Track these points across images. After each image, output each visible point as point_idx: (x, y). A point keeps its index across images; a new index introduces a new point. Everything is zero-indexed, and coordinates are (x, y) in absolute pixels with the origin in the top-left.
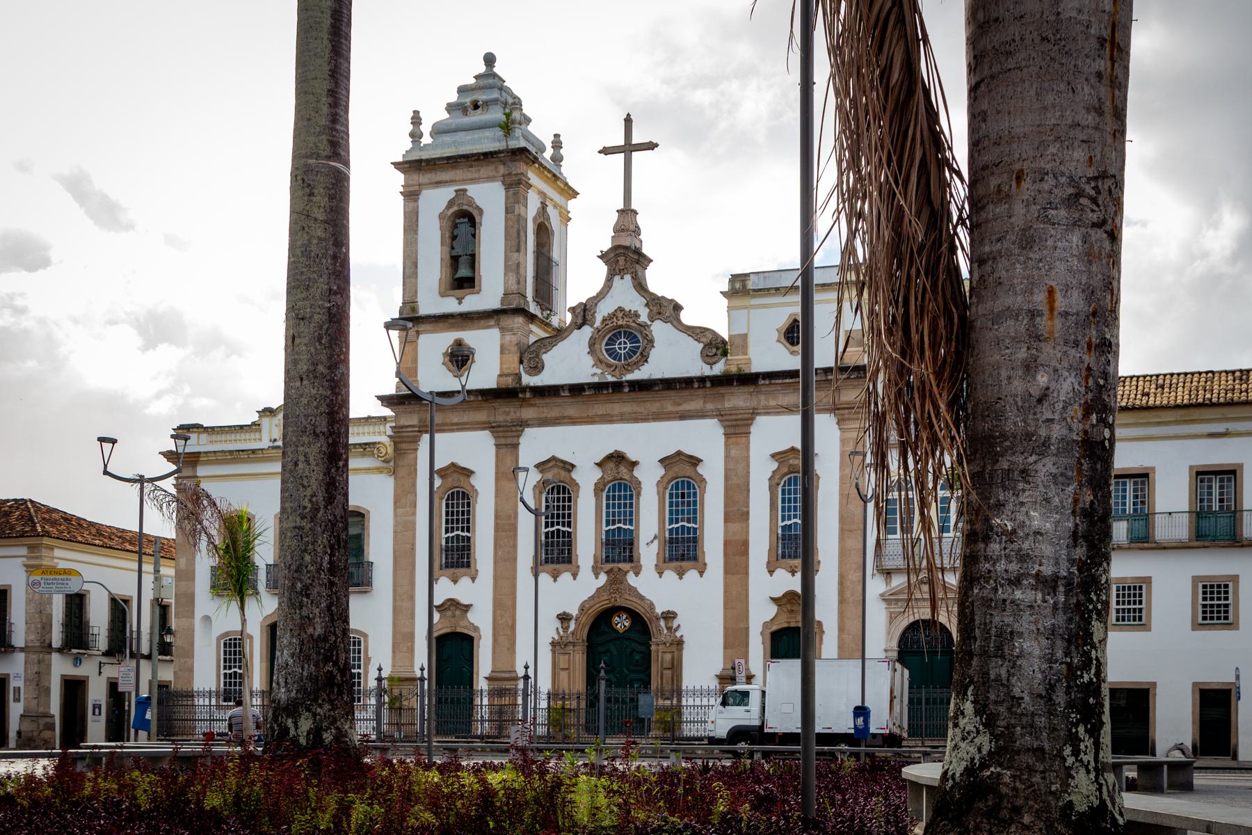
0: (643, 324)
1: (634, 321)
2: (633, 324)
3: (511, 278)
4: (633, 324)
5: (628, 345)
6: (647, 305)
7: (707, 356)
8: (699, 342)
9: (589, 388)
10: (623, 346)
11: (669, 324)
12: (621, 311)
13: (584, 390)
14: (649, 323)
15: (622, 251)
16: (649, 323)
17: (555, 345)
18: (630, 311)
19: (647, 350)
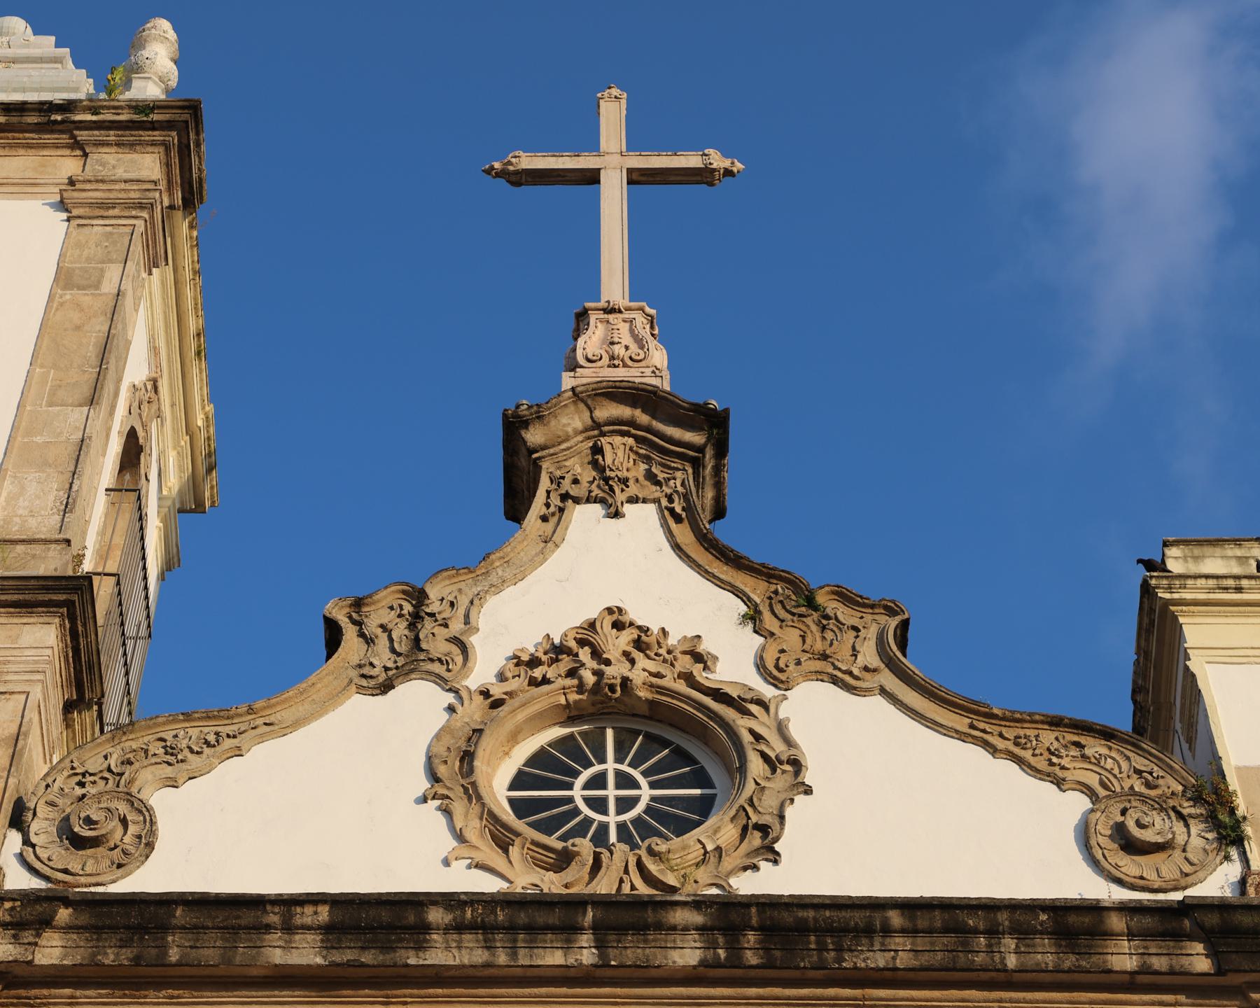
0: (734, 694)
1: (688, 678)
2: (681, 687)
3: (32, 488)
4: (681, 687)
5: (646, 793)
6: (753, 618)
7: (1132, 846)
8: (1059, 783)
9: (459, 927)
10: (611, 793)
11: (878, 701)
12: (618, 626)
13: (419, 933)
14: (768, 692)
15: (624, 411)
16: (768, 692)
17: (238, 753)
18: (664, 632)
19: (769, 802)
